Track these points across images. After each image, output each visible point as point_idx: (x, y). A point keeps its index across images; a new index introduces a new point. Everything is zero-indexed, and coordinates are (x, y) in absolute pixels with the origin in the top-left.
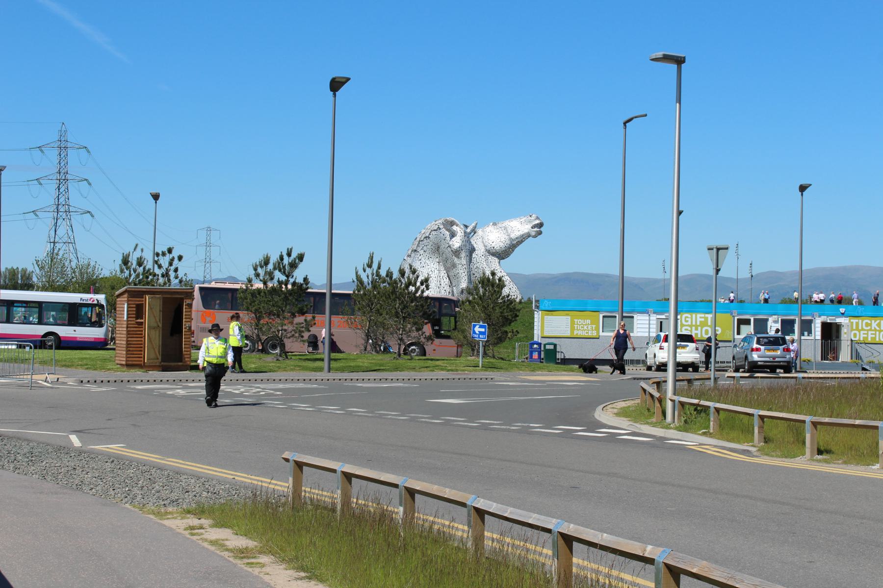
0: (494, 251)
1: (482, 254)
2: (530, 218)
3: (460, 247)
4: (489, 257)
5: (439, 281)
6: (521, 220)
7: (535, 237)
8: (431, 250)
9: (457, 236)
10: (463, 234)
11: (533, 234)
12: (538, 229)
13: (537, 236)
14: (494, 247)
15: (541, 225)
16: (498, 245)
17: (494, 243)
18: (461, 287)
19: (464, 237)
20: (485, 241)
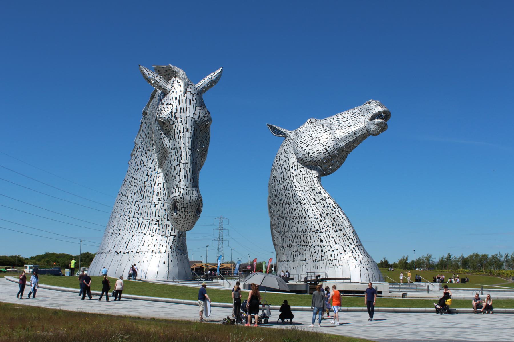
0: (309, 159)
1: (291, 166)
2: (368, 105)
3: (171, 113)
4: (302, 169)
5: (156, 193)
6: (355, 111)
7: (376, 133)
8: (148, 135)
9: (171, 92)
10: (182, 88)
11: (373, 128)
12: (380, 120)
13: (378, 133)
14: (309, 153)
15: (385, 116)
16: (314, 150)
17: (309, 147)
18: (172, 196)
19: (182, 93)
20: (296, 146)
